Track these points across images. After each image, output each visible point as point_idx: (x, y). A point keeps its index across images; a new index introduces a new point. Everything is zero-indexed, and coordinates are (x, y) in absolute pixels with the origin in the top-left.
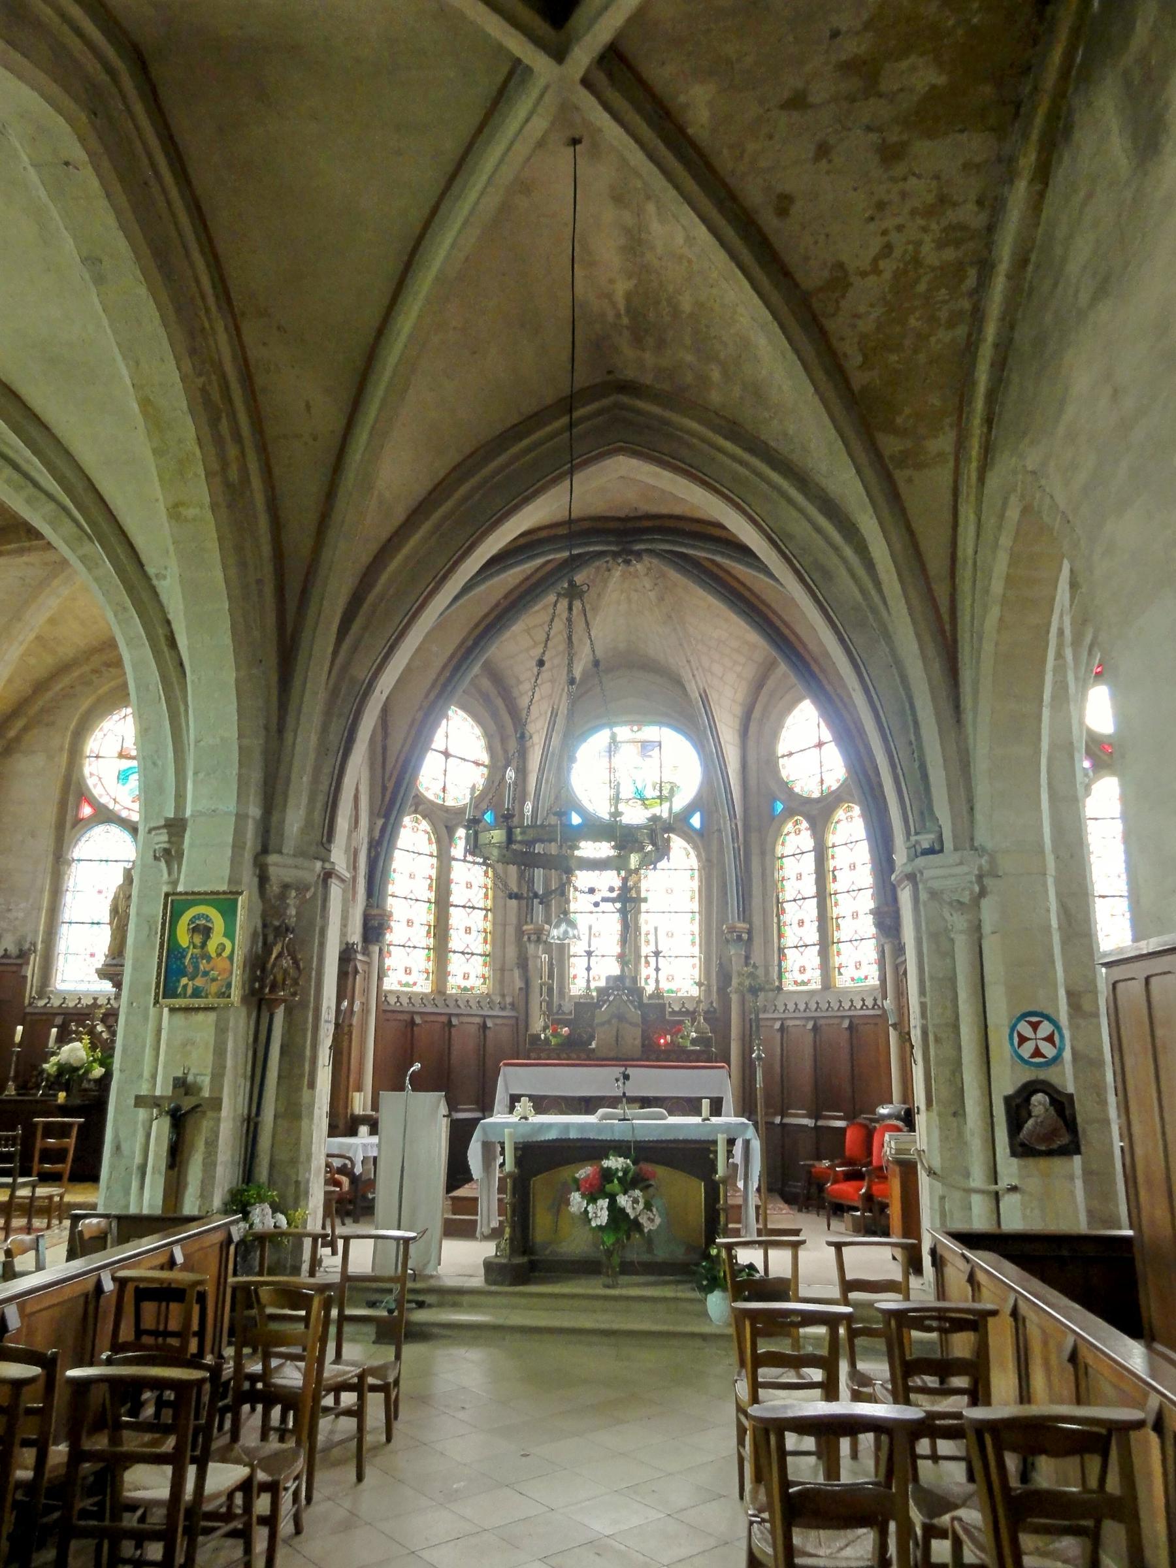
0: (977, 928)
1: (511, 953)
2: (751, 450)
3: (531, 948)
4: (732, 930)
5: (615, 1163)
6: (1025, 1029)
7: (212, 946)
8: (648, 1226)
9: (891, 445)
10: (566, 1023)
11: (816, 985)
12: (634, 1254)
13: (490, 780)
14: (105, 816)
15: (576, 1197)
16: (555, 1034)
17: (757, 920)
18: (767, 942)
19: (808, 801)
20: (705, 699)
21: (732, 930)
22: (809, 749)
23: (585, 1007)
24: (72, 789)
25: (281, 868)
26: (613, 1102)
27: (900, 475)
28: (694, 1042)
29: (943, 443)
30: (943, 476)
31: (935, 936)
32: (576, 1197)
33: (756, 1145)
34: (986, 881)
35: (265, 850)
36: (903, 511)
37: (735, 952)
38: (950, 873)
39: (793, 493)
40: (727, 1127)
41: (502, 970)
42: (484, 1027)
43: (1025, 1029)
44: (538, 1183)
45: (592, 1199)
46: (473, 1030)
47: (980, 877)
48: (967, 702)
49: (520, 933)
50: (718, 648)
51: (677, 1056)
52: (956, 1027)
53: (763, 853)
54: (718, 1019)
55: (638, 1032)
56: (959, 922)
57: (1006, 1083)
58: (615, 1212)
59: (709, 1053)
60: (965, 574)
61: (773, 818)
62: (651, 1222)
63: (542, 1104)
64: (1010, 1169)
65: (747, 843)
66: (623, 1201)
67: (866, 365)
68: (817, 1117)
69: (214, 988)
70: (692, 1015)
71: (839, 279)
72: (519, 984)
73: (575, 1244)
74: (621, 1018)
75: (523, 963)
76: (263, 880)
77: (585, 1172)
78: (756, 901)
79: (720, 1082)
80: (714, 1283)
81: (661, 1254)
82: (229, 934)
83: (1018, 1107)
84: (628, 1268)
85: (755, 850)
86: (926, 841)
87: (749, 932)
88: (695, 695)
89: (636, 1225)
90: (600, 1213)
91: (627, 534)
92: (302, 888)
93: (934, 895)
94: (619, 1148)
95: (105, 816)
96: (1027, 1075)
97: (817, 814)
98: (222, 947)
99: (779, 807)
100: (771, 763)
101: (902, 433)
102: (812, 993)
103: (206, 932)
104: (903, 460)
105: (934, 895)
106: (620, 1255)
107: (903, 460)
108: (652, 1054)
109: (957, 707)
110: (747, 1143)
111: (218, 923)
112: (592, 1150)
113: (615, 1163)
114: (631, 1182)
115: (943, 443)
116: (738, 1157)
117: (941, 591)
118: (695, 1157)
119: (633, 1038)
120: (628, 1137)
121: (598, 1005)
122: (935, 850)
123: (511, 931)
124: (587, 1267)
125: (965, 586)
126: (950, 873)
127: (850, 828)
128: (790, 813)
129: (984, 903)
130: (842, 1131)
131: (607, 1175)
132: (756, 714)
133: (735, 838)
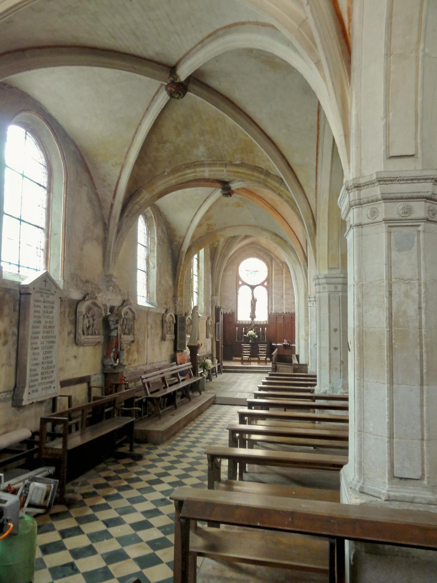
14: (244, 284)
24: (238, 278)
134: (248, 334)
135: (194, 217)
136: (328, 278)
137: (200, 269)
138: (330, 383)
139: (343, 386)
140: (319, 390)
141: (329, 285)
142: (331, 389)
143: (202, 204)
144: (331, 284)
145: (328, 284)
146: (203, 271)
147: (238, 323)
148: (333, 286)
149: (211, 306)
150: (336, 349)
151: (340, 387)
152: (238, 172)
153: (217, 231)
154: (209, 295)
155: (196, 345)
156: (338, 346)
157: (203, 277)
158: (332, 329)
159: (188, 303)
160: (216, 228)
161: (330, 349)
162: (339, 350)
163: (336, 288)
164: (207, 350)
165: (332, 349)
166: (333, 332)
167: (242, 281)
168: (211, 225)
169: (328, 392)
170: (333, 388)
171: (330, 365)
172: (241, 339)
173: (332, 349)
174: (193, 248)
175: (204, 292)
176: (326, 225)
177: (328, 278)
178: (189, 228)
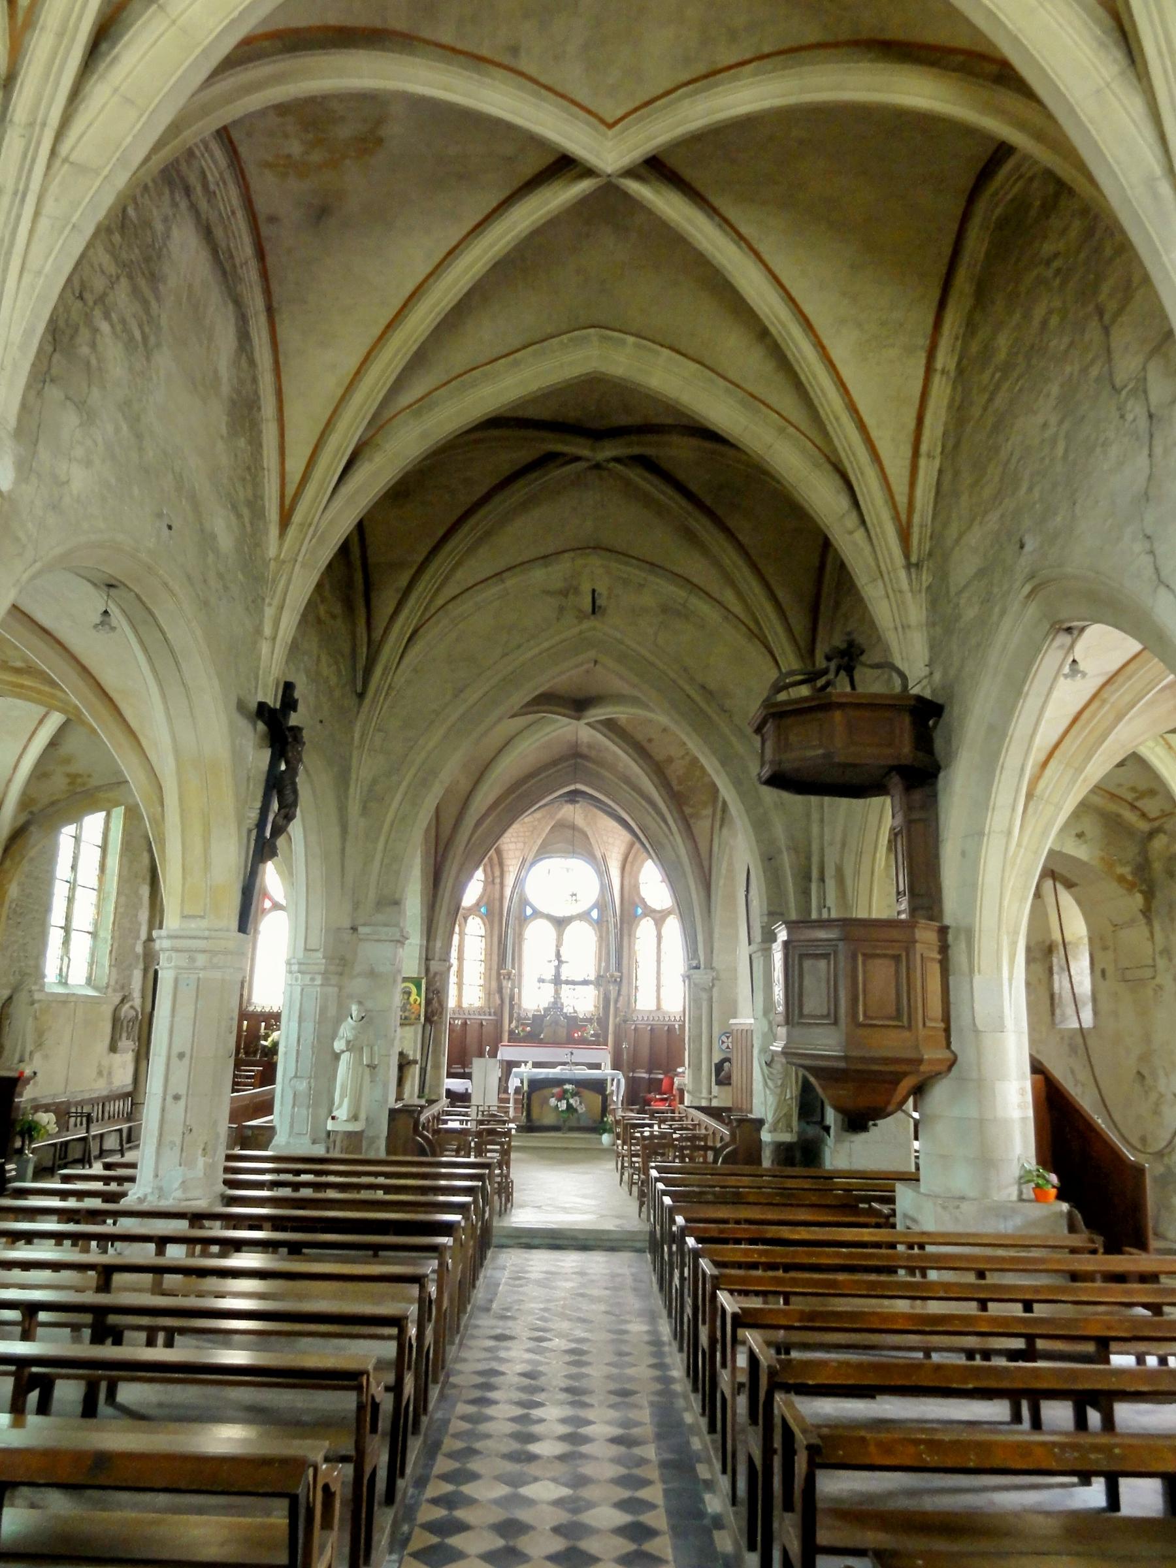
0: (711, 999)
1: (494, 984)
2: (633, 790)
3: (505, 983)
4: (612, 976)
5: (568, 1087)
6: (724, 1039)
7: (412, 1000)
8: (580, 1111)
9: (688, 810)
10: (528, 1025)
11: (654, 1008)
12: (574, 1123)
13: (485, 889)
15: (553, 1101)
16: (523, 1030)
17: (625, 971)
18: (630, 983)
19: (654, 911)
20: (604, 858)
21: (612, 976)
22: (654, 887)
23: (538, 1019)
25: (435, 966)
26: (564, 1064)
27: (692, 821)
28: (592, 1036)
29: (708, 812)
30: (707, 824)
31: (695, 1000)
32: (553, 1101)
33: (623, 1081)
34: (716, 982)
35: (427, 959)
36: (692, 834)
37: (613, 989)
38: (702, 977)
39: (650, 810)
40: (611, 1075)
41: (489, 994)
42: (482, 1024)
43: (724, 1039)
44: (534, 1096)
45: (559, 1100)
46: (476, 1026)
47: (713, 979)
48: (713, 909)
49: (499, 974)
50: (613, 839)
51: (583, 1042)
52: (700, 1036)
53: (630, 935)
54: (602, 1022)
55: (565, 1031)
56: (704, 996)
57: (716, 1059)
58: (569, 1106)
59: (599, 1041)
60: (714, 859)
61: (636, 917)
62: (582, 1109)
63: (536, 1065)
64: (715, 1089)
65: (621, 929)
66: (571, 1101)
67: (680, 783)
68: (650, 1072)
69: (413, 1017)
70: (590, 1020)
71: (670, 760)
72: (498, 1002)
73: (549, 1119)
74: (556, 1023)
75: (500, 990)
76: (427, 970)
77: (556, 1090)
78: (625, 962)
79: (604, 1056)
80: (605, 1131)
81: (583, 1123)
82: (419, 994)
83: (719, 1067)
84: (571, 1129)
85: (626, 931)
86: (694, 963)
87: (621, 978)
88: (599, 856)
89: (576, 1110)
90: (563, 1105)
91: (576, 792)
92: (441, 974)
93: (695, 985)
94: (570, 1081)
95: (276, 906)
96: (722, 1056)
97: (659, 918)
98: (416, 1001)
99: (640, 911)
100: (636, 887)
101: (692, 807)
102: (651, 1012)
103: (409, 994)
104: (692, 816)
105: (695, 985)
106: (569, 1123)
107: (692, 816)
108: (570, 1041)
109: (709, 911)
110: (619, 1080)
111: (414, 990)
112: (559, 1082)
113: (568, 1087)
114: (574, 1095)
115: (708, 812)
116: (614, 1088)
117: (706, 864)
118: (598, 1086)
119: (562, 1033)
120: (572, 1077)
121: (545, 1016)
122: (697, 968)
123: (494, 973)
124: (555, 1128)
125: (714, 865)
126: (702, 977)
127: (673, 926)
128: (645, 915)
129: (715, 990)
130: (661, 1080)
131: (566, 1091)
132: (630, 859)
133: (615, 926)
134: (270, 1039)
135: (21, 756)
136: (176, 937)
137: (108, 871)
138: (156, 1176)
139: (183, 1182)
140: (136, 1195)
141: (179, 954)
142: (156, 1191)
143: (36, 729)
144: (181, 951)
145: (177, 950)
146: (116, 878)
147: (251, 1009)
148: (186, 955)
149: (141, 966)
150: (177, 1098)
151: (176, 1185)
152: (22, 686)
153: (98, 788)
154: (138, 938)
155: (14, 1074)
156: (182, 1091)
157: (114, 894)
158: (175, 1052)
159: (32, 963)
160: (94, 782)
161: (164, 1099)
162: (182, 1102)
163: (192, 960)
164: (110, 1083)
165: (169, 1099)
166: (174, 1060)
167: (271, 899)
168: (80, 776)
169: (149, 1198)
170: (160, 1189)
171: (161, 1135)
172: (255, 1054)
173: (169, 1099)
174: (33, 828)
175: (113, 931)
176: (177, 819)
177: (176, 937)
178: (10, 781)
